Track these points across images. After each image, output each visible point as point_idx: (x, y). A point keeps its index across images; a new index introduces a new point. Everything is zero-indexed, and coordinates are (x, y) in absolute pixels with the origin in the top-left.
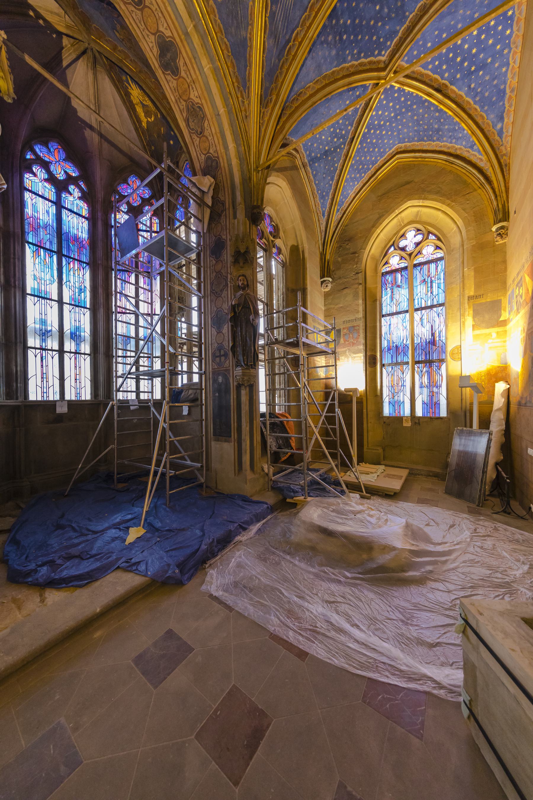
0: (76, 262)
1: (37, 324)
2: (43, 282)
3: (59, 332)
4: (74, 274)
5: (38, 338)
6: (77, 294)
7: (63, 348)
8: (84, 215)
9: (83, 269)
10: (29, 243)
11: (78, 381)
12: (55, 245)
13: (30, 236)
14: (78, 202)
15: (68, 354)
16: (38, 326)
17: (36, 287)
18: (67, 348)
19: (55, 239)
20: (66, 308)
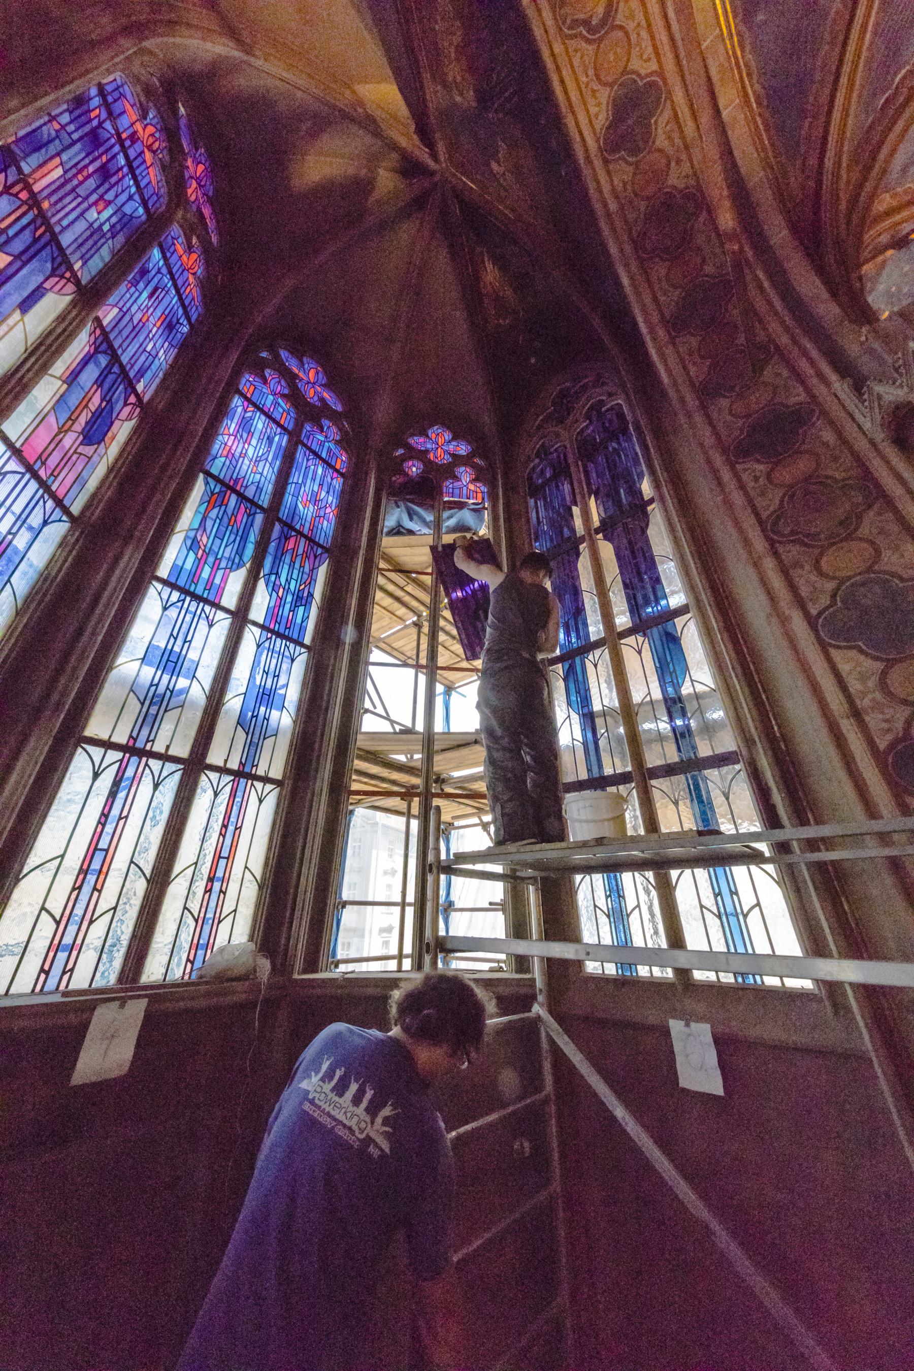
0: (303, 540)
1: (150, 664)
2: (211, 559)
3: (209, 698)
4: (293, 562)
5: (134, 705)
6: (288, 606)
7: (204, 755)
8: (338, 467)
9: (315, 557)
10: (208, 474)
11: (217, 886)
12: (267, 497)
13: (220, 462)
14: (332, 446)
15: (214, 776)
16: (148, 672)
17: (188, 566)
18: (215, 757)
19: (271, 487)
20: (251, 637)
